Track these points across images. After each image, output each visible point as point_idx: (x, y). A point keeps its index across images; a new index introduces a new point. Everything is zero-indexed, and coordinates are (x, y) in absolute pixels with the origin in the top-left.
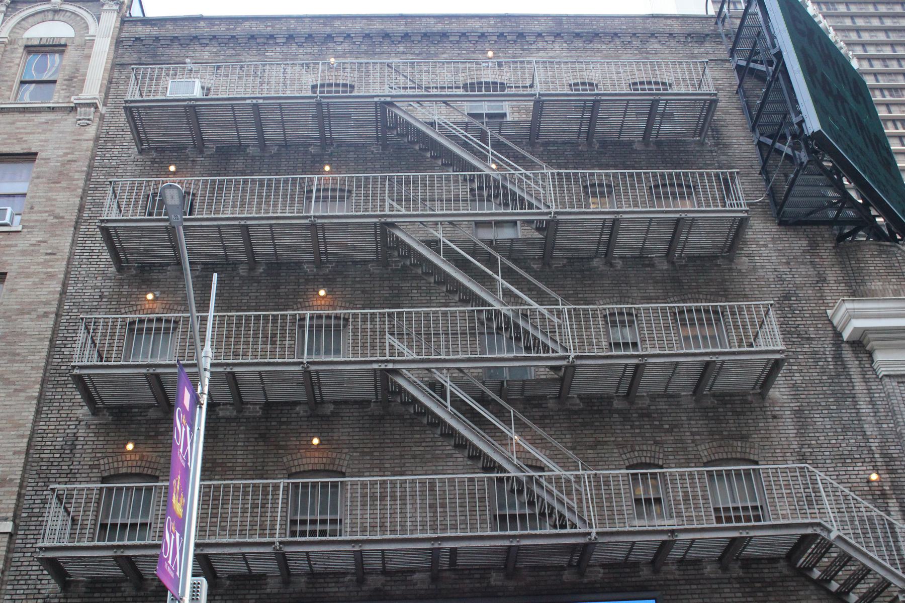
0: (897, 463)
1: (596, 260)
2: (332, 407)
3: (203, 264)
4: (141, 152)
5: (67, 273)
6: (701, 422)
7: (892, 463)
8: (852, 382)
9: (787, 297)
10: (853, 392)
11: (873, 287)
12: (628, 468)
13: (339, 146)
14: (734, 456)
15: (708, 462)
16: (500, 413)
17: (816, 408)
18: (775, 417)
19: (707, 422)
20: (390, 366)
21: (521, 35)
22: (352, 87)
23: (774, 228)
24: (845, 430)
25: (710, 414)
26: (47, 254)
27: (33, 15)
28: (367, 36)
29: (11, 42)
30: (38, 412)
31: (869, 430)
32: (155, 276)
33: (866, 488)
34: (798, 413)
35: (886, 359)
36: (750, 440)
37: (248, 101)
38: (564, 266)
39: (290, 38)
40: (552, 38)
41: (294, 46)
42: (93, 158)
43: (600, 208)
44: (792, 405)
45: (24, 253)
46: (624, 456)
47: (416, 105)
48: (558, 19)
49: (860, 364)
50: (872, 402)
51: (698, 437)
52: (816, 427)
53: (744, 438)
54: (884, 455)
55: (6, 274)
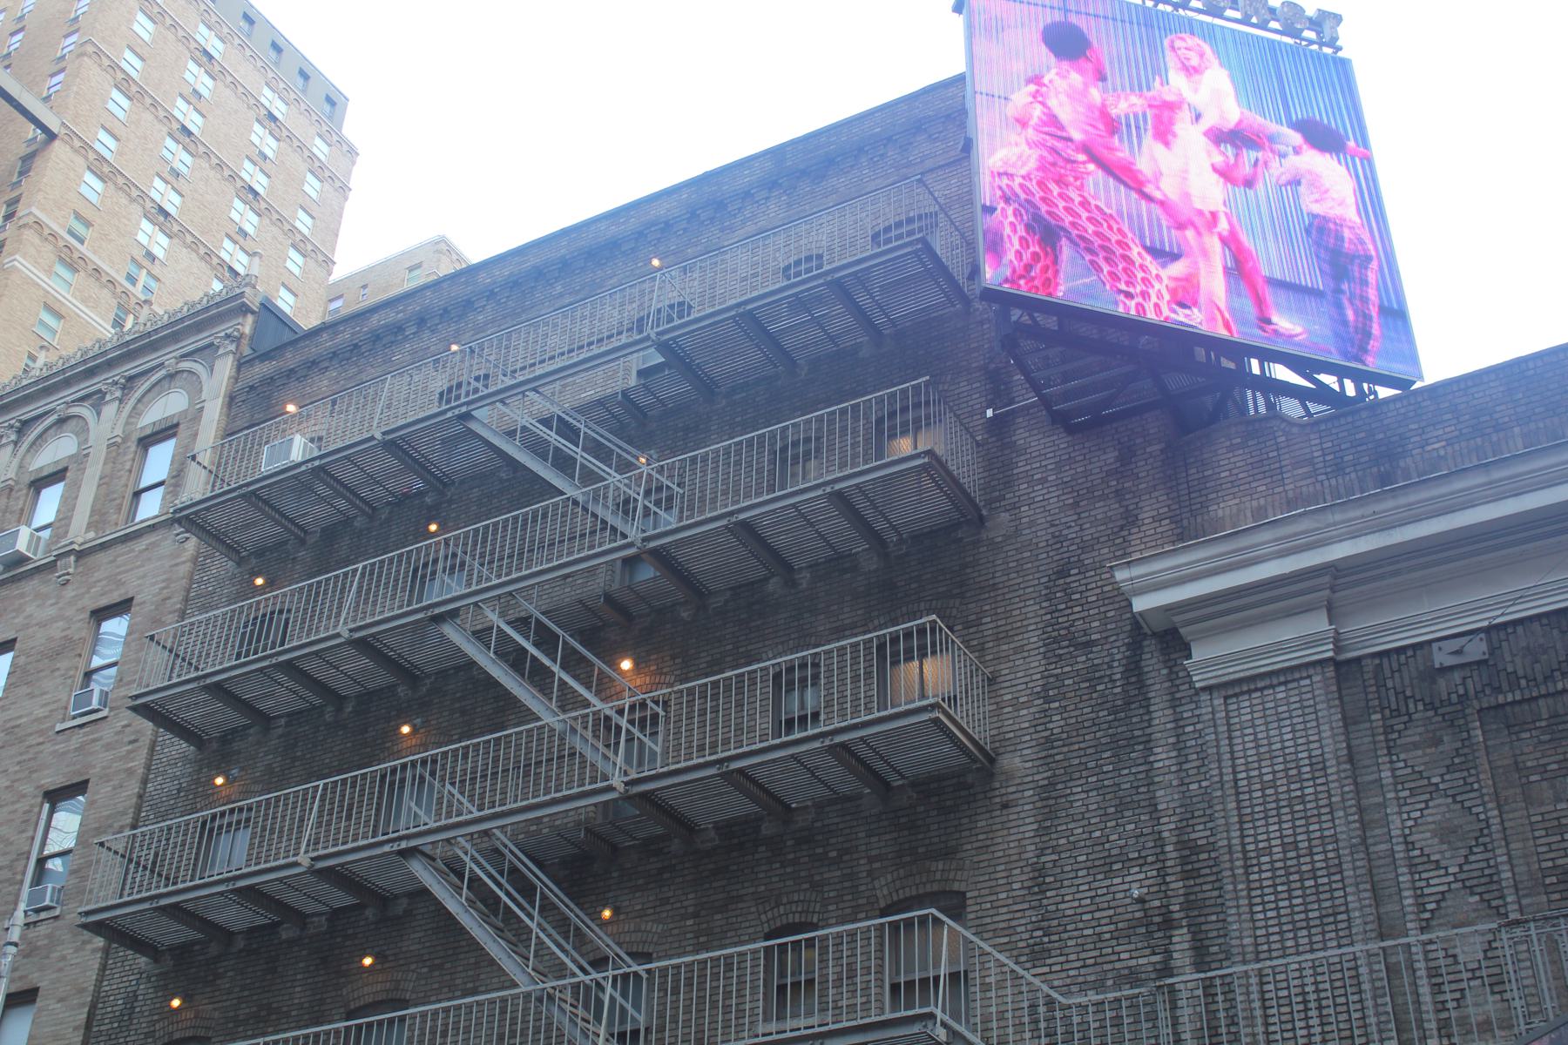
0: (1203, 856)
1: (774, 580)
2: (404, 902)
3: (289, 715)
4: (239, 564)
5: (148, 768)
6: (888, 837)
7: (1194, 858)
8: (1149, 713)
9: (1063, 573)
10: (1148, 731)
11: (1220, 513)
12: (767, 938)
13: (462, 482)
14: (928, 888)
15: (888, 906)
16: (527, 890)
17: (1077, 775)
18: (1005, 806)
19: (895, 835)
20: (404, 845)
21: (720, 205)
22: (820, 257)
23: (1062, 440)
24: (1121, 807)
25: (903, 820)
26: (131, 742)
27: (149, 390)
29: (125, 440)
30: (103, 968)
31: (1166, 799)
32: (236, 746)
33: (1138, 915)
34: (1047, 791)
35: (1211, 656)
36: (959, 856)
37: (303, 468)
38: (727, 601)
40: (764, 194)
41: (427, 333)
42: (188, 591)
43: (817, 478)
44: (1037, 777)
45: (108, 747)
46: (763, 917)
47: (531, 394)
48: (776, 154)
49: (1171, 672)
50: (1179, 746)
51: (877, 865)
52: (1072, 811)
53: (949, 853)
54: (1181, 845)
55: (86, 782)
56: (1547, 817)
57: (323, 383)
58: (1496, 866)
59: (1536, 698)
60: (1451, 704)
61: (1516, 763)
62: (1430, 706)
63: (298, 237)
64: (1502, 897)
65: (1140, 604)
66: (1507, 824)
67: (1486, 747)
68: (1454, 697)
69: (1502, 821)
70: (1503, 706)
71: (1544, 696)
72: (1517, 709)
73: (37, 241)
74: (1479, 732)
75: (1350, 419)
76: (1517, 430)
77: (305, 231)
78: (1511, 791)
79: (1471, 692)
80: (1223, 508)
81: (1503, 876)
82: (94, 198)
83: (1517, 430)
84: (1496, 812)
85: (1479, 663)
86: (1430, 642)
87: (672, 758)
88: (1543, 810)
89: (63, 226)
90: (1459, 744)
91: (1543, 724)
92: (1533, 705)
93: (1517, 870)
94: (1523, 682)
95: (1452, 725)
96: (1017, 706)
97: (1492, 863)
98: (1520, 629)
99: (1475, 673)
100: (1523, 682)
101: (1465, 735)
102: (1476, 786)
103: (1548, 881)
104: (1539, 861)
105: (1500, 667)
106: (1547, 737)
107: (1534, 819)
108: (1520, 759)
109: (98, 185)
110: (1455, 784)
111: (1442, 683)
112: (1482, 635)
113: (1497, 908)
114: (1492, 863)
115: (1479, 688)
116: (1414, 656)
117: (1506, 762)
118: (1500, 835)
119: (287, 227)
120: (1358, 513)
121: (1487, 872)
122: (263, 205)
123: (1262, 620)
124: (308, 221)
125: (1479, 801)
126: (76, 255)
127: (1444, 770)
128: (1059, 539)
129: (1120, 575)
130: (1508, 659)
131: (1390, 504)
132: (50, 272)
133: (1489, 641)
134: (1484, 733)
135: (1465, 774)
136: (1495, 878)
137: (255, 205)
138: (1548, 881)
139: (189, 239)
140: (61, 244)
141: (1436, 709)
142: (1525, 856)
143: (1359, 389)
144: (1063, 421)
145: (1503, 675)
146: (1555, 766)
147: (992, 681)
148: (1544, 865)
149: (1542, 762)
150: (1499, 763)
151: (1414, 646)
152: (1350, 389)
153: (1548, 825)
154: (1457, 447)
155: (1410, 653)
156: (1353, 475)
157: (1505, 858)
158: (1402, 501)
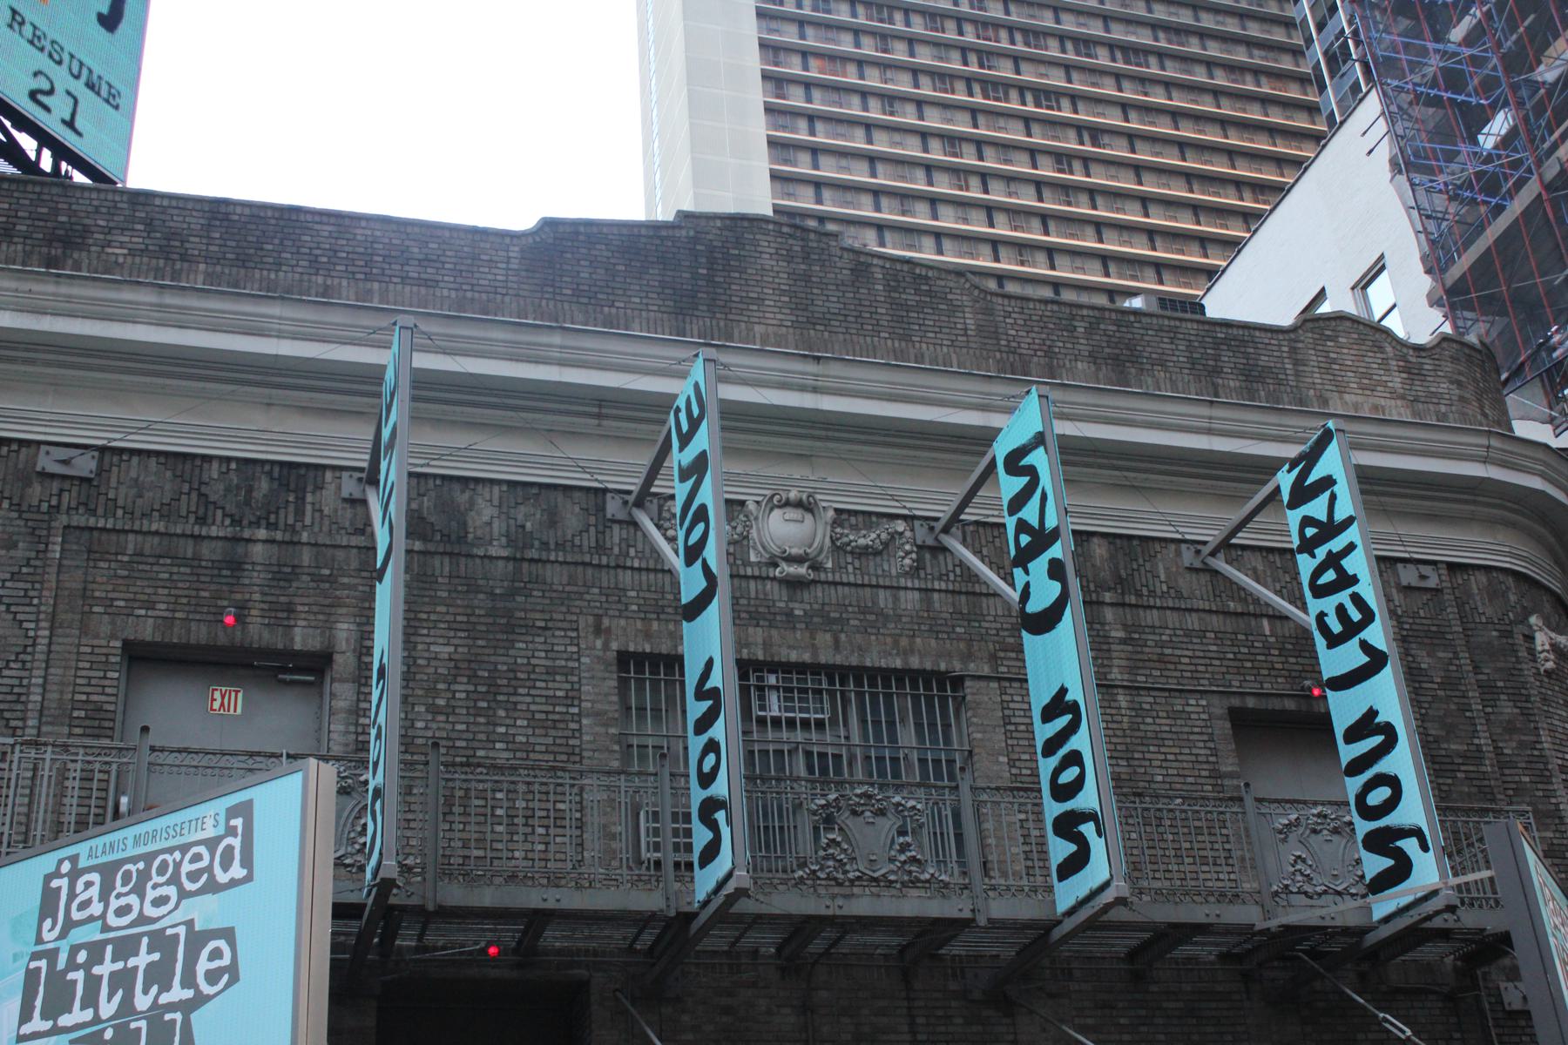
56: (97, 650)
58: (28, 686)
59: (127, 532)
60: (38, 512)
61: (85, 589)
62: (16, 506)
64: (24, 719)
66: (53, 648)
67: (60, 565)
68: (45, 506)
69: (50, 644)
70: (91, 529)
71: (136, 532)
72: (104, 537)
74: (58, 548)
75: (38, 189)
76: (202, 267)
78: (70, 616)
79: (64, 506)
81: (32, 698)
83: (202, 267)
84: (47, 633)
85: (82, 480)
86: (39, 443)
88: (95, 642)
90: (33, 554)
91: (126, 559)
92: (122, 537)
93: (48, 696)
94: (120, 512)
95: (32, 534)
97: (25, 682)
98: (135, 460)
99: (75, 490)
100: (120, 512)
101: (42, 547)
102: (35, 601)
103: (76, 714)
104: (74, 693)
105: (103, 490)
106: (126, 573)
107: (83, 649)
108: (90, 586)
110: (14, 593)
111: (36, 491)
112: (96, 454)
113: (15, 728)
114: (25, 682)
115: (73, 504)
116: (17, 452)
117: (74, 585)
118: (43, 657)
120: (13, 284)
121: (16, 690)
125: (33, 617)
127: (8, 576)
130: (113, 483)
131: (51, 288)
133: (101, 460)
134: (63, 550)
135: (29, 586)
136: (23, 698)
138: (76, 714)
141: (21, 512)
142: (62, 684)
143: (56, 167)
145: (102, 499)
146: (122, 603)
148: (78, 697)
149: (110, 595)
150: (67, 585)
151: (21, 442)
152: (46, 163)
153: (94, 658)
154: (137, 260)
155: (14, 447)
156: (20, 247)
157: (40, 681)
158: (64, 290)
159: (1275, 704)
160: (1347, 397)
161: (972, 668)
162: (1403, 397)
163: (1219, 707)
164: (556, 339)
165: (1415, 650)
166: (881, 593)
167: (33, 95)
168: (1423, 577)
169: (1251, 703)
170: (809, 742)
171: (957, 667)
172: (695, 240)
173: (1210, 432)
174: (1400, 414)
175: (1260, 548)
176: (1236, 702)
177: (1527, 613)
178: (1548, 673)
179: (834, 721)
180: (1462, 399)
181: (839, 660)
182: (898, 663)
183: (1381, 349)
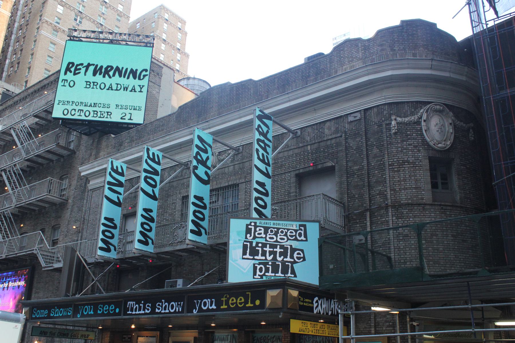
28: (32, 93)
35: (93, 183)
39: (20, 100)
57: (7, 112)
63: (119, 12)
65: (82, 174)
73: (46, 26)
77: (121, 10)
80: (102, 154)
82: (61, 12)
87: (33, 198)
89: (53, 21)
96: (72, 190)
109: (62, 8)
119: (115, 10)
122: (108, 5)
123: (96, 178)
124: (122, 7)
126: (57, 28)
128: (83, 158)
129: (79, 169)
132: (50, 33)
137: (106, 5)
139: (88, 18)
140: (53, 25)
144: (85, 134)
147: (70, 185)
159: (307, 169)
160: (344, 67)
161: (241, 181)
162: (362, 59)
163: (293, 174)
164: (168, 137)
165: (349, 140)
166: (226, 169)
167: (121, 118)
168: (355, 117)
169: (301, 171)
170: (213, 206)
171: (238, 182)
172: (202, 99)
173: (290, 101)
174: (359, 66)
175: (311, 125)
176: (297, 172)
177: (390, 115)
178: (395, 133)
179: (215, 202)
180: (382, 50)
181: (217, 187)
182: (227, 184)
183: (357, 46)
